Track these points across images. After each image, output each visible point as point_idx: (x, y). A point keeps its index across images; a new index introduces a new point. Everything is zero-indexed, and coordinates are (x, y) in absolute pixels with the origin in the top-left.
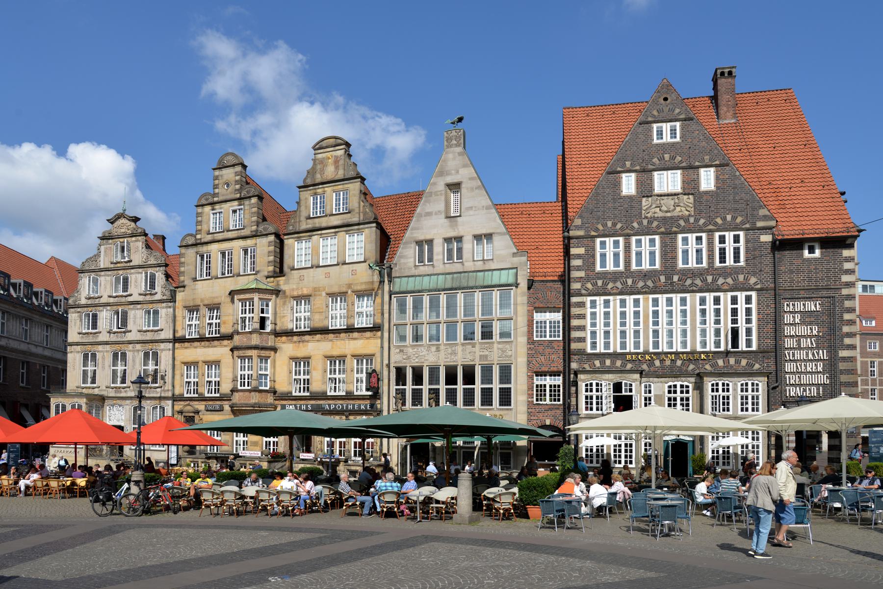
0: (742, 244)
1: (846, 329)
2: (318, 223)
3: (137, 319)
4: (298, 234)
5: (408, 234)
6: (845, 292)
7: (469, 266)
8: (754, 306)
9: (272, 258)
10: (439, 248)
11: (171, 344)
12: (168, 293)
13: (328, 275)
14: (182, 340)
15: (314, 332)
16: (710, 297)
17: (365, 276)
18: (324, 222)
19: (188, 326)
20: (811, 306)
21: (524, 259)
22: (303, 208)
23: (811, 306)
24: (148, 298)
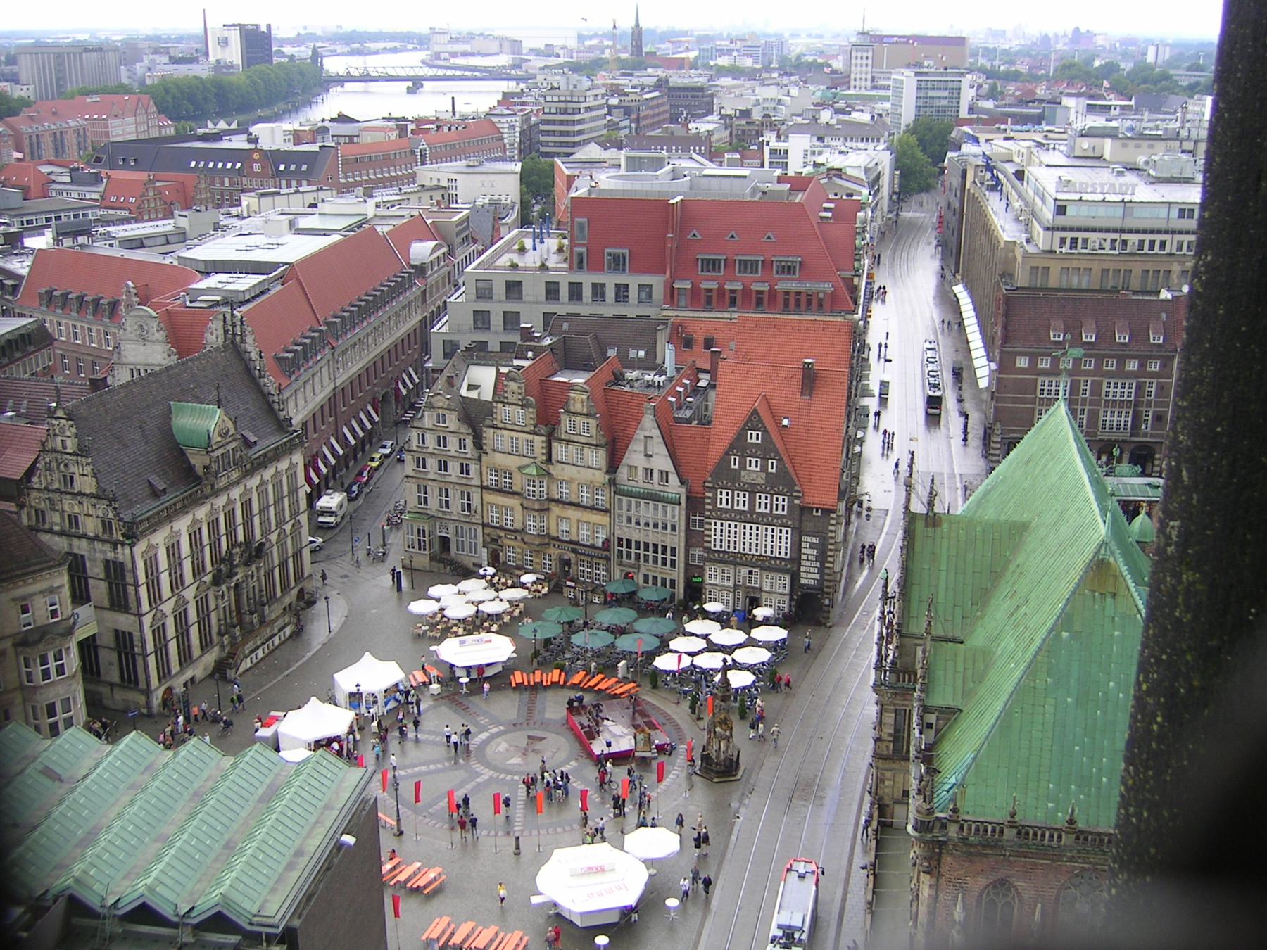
0: (786, 503)
1: (829, 553)
2: (572, 438)
3: (454, 468)
4: (560, 440)
5: (624, 460)
6: (830, 534)
7: (656, 487)
8: (789, 536)
9: (544, 451)
10: (640, 472)
11: (479, 490)
12: (476, 455)
13: (579, 472)
14: (487, 488)
15: (571, 504)
16: (770, 528)
17: (601, 477)
18: (576, 438)
19: (489, 479)
20: (815, 540)
21: (684, 490)
22: (562, 425)
23: (815, 540)
24: (462, 455)
